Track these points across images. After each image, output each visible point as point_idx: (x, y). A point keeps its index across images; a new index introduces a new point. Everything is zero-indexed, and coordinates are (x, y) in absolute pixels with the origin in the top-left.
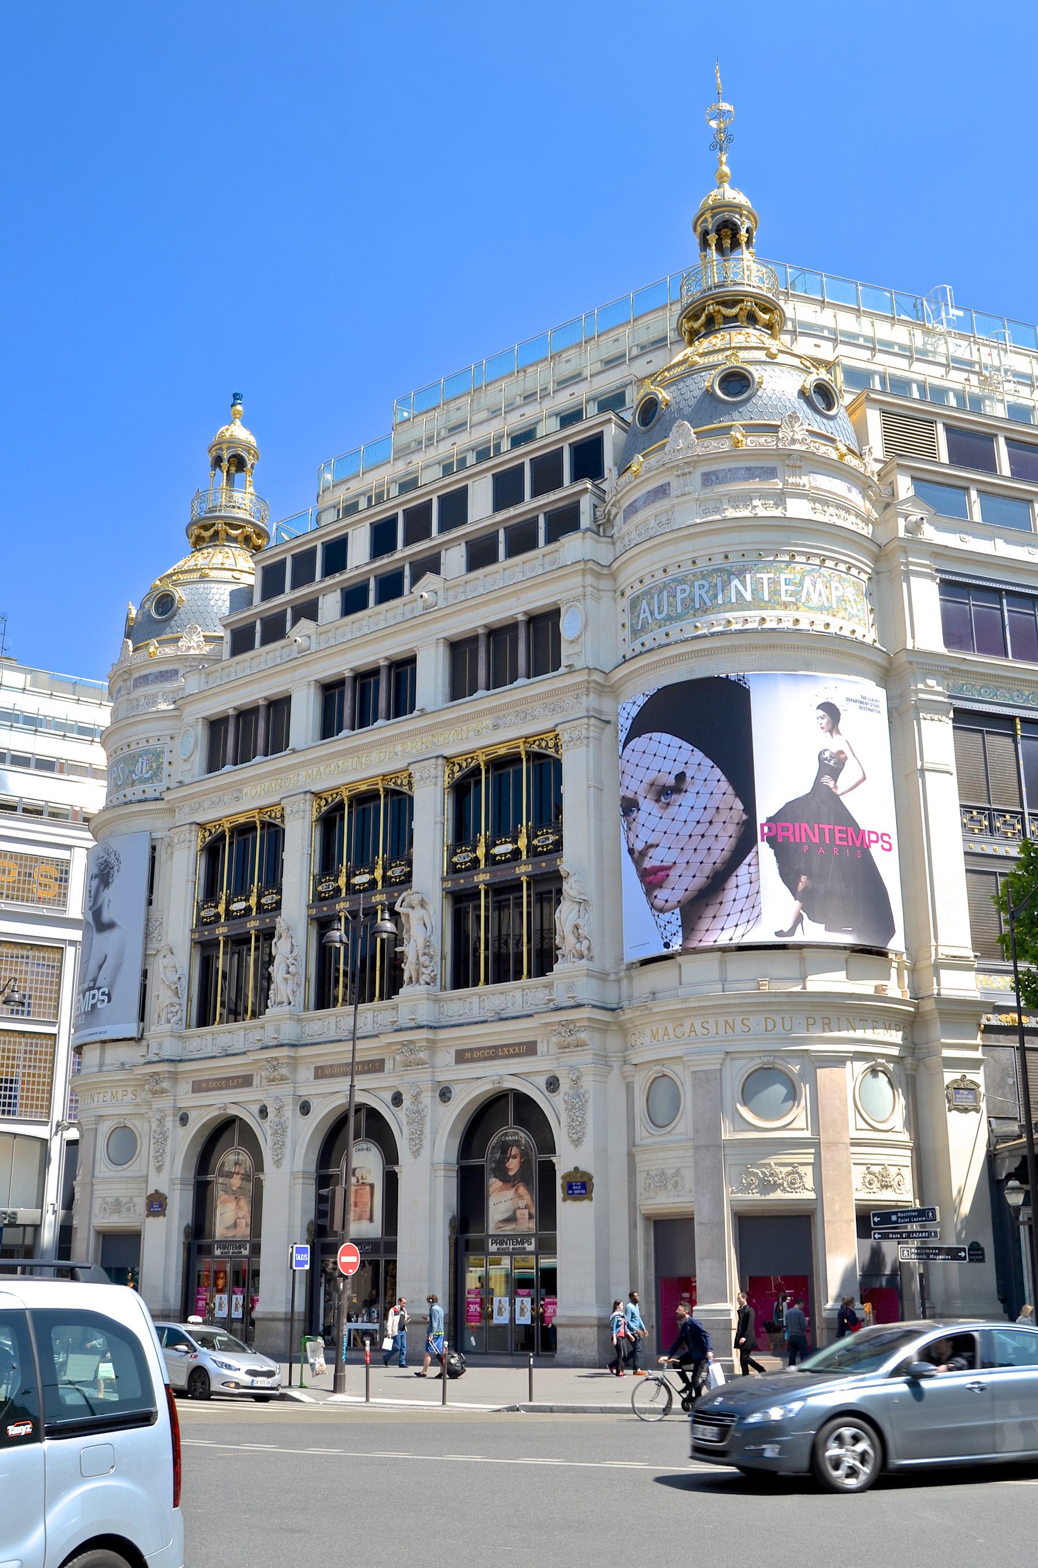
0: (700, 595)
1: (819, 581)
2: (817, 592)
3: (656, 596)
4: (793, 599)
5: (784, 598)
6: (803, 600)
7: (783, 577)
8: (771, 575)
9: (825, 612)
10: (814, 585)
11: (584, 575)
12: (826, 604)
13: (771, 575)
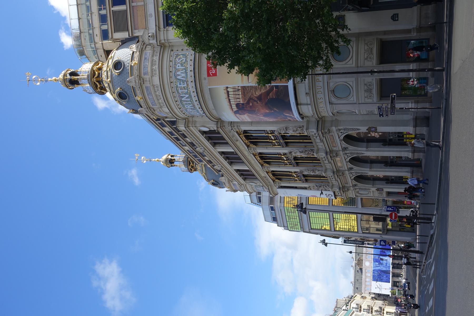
1: (177, 73)
2: (181, 74)
4: (185, 82)
5: (185, 85)
6: (185, 79)
7: (179, 86)
8: (179, 89)
9: (187, 71)
10: (179, 75)
11: (189, 126)
12: (184, 71)
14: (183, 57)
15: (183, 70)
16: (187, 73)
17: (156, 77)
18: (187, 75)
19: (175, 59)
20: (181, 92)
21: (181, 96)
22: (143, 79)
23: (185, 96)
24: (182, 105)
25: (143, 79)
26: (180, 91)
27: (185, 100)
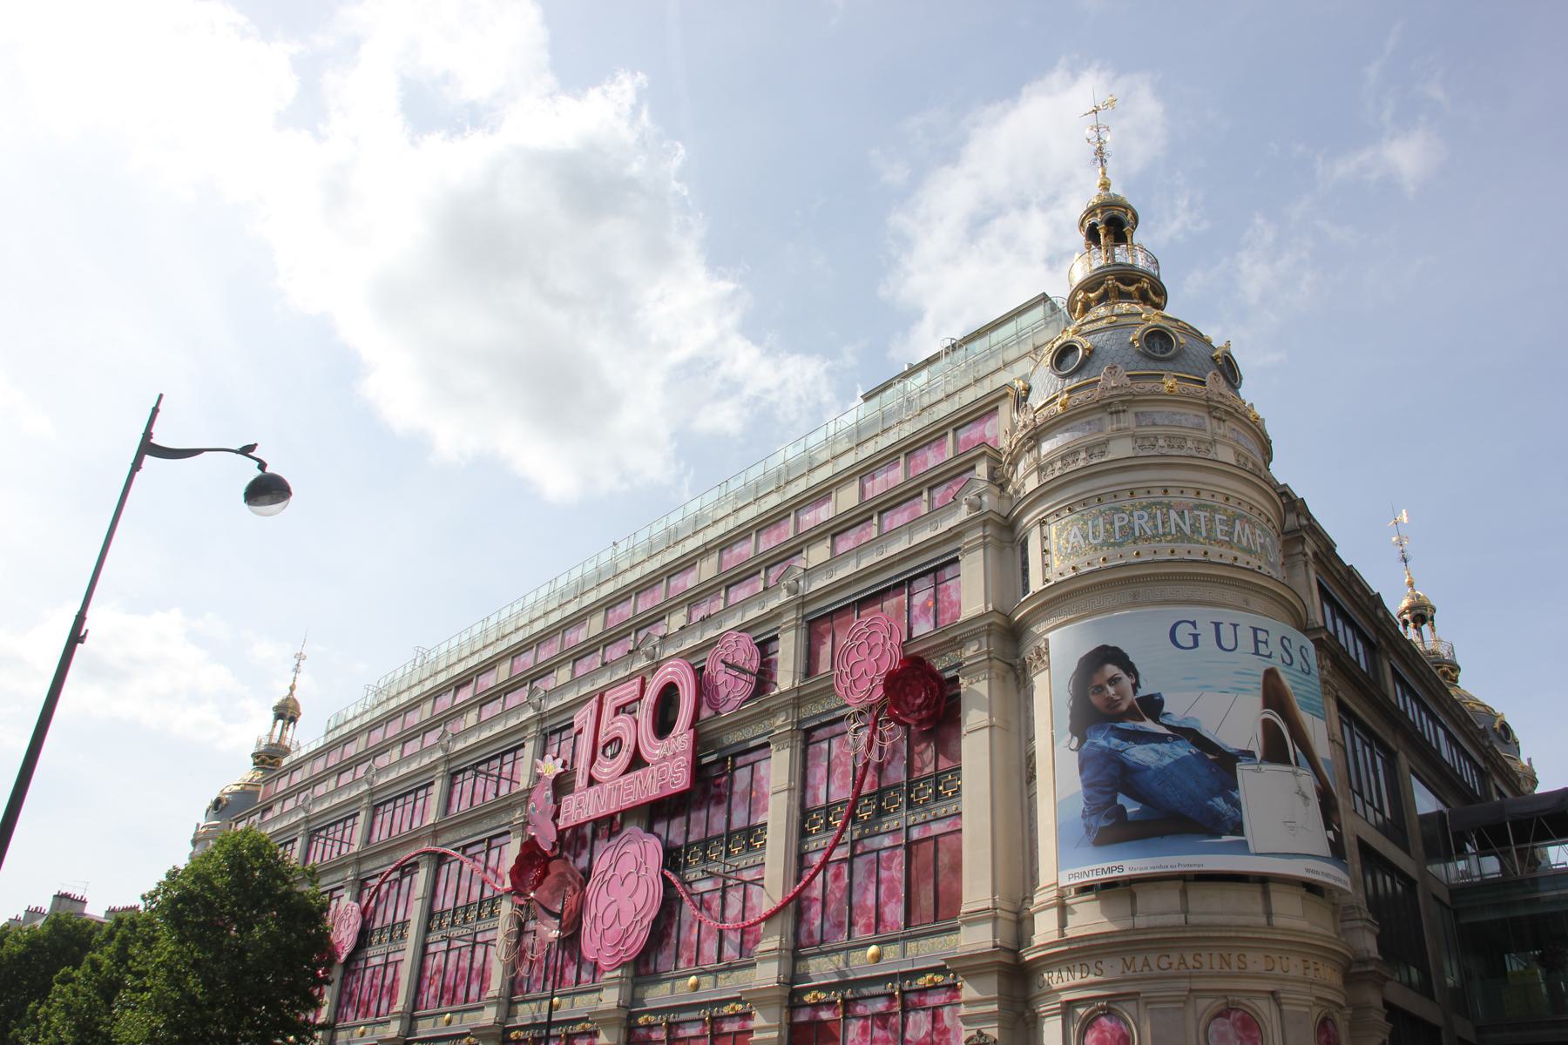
0: (1140, 525)
3: (1090, 523)
4: (1227, 539)
9: (1253, 556)
17: (1133, 449)
20: (1220, 519)
21: (1186, 512)
22: (1124, 411)
24: (1149, 506)
25: (1124, 411)
27: (1172, 520)
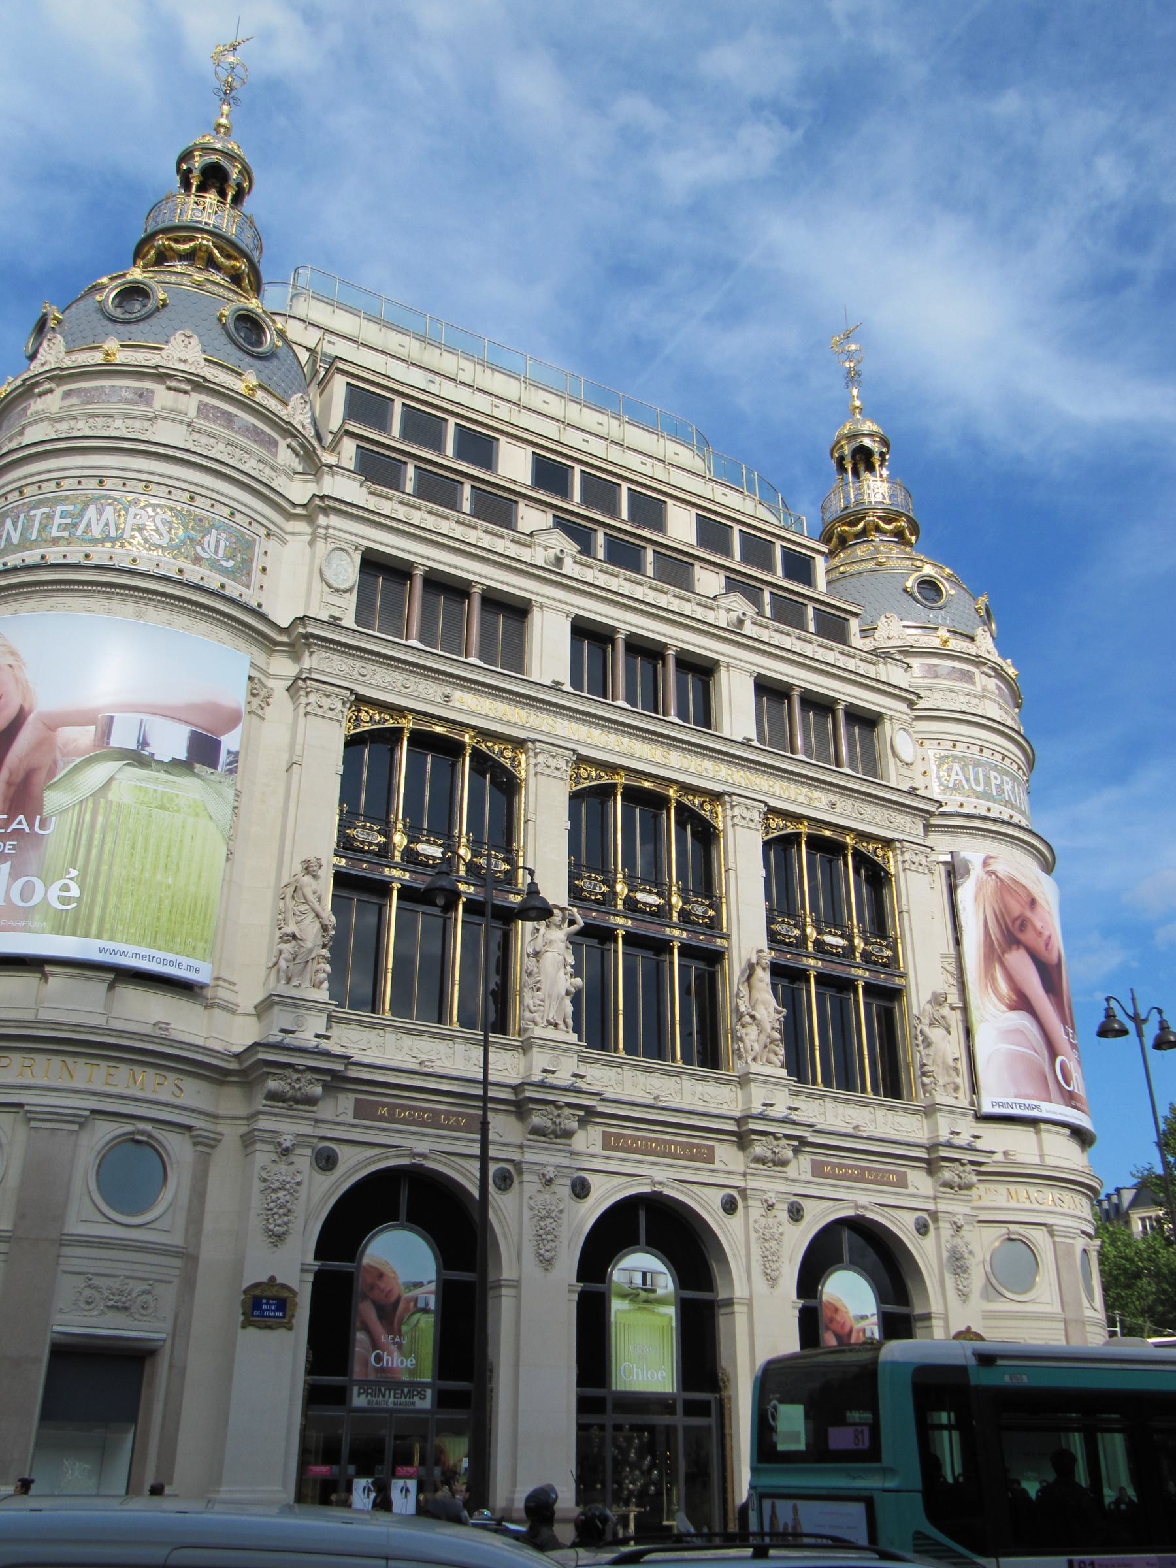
1: (109, 509)
4: (66, 534)
5: (55, 533)
6: (79, 533)
7: (59, 509)
8: (46, 510)
9: (109, 545)
10: (100, 512)
12: (113, 534)
13: (46, 510)
14: (172, 539)
15: (117, 529)
16: (100, 545)
18: (94, 541)
19: (171, 509)
21: (22, 516)
23: (15, 529)
26: (38, 513)
